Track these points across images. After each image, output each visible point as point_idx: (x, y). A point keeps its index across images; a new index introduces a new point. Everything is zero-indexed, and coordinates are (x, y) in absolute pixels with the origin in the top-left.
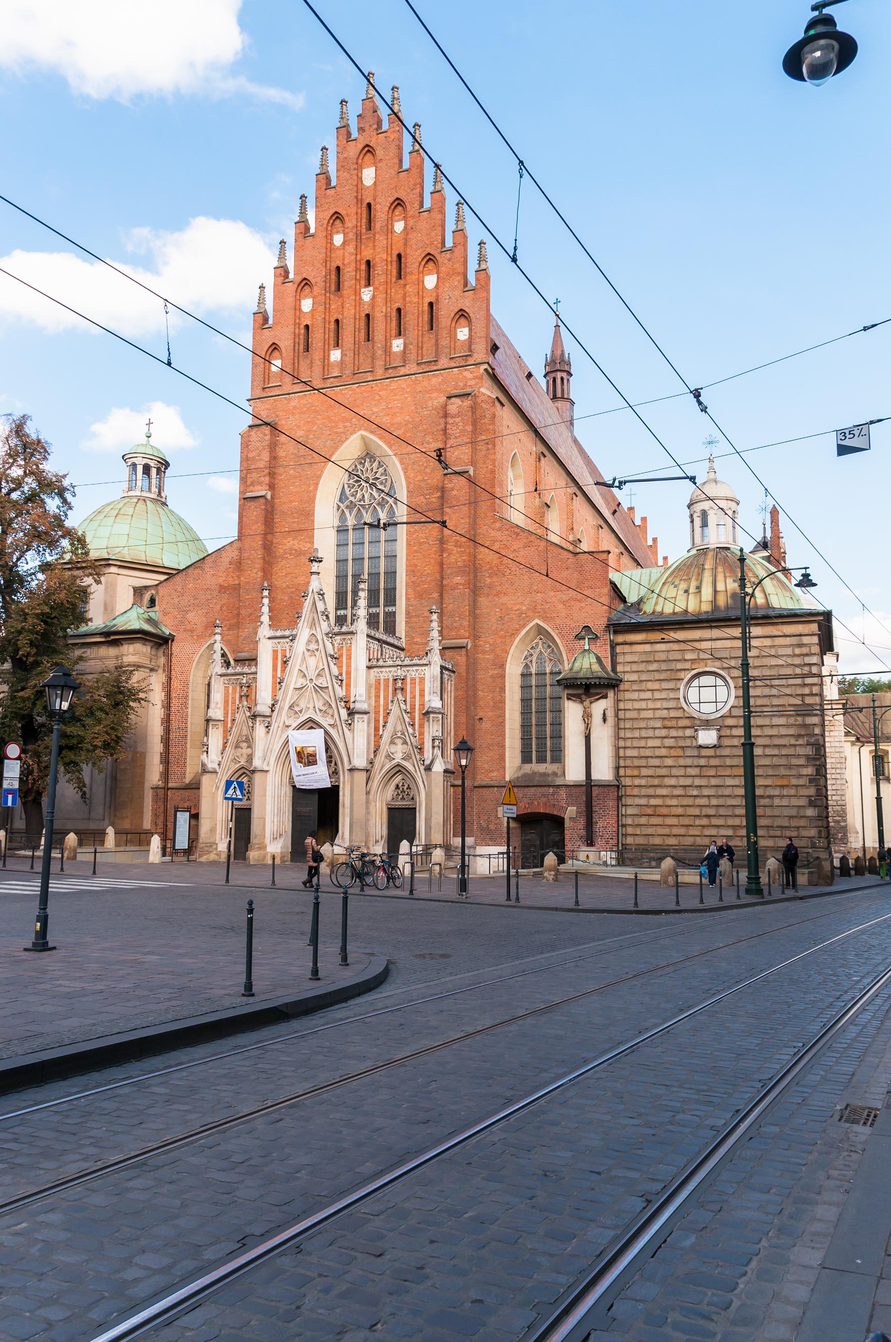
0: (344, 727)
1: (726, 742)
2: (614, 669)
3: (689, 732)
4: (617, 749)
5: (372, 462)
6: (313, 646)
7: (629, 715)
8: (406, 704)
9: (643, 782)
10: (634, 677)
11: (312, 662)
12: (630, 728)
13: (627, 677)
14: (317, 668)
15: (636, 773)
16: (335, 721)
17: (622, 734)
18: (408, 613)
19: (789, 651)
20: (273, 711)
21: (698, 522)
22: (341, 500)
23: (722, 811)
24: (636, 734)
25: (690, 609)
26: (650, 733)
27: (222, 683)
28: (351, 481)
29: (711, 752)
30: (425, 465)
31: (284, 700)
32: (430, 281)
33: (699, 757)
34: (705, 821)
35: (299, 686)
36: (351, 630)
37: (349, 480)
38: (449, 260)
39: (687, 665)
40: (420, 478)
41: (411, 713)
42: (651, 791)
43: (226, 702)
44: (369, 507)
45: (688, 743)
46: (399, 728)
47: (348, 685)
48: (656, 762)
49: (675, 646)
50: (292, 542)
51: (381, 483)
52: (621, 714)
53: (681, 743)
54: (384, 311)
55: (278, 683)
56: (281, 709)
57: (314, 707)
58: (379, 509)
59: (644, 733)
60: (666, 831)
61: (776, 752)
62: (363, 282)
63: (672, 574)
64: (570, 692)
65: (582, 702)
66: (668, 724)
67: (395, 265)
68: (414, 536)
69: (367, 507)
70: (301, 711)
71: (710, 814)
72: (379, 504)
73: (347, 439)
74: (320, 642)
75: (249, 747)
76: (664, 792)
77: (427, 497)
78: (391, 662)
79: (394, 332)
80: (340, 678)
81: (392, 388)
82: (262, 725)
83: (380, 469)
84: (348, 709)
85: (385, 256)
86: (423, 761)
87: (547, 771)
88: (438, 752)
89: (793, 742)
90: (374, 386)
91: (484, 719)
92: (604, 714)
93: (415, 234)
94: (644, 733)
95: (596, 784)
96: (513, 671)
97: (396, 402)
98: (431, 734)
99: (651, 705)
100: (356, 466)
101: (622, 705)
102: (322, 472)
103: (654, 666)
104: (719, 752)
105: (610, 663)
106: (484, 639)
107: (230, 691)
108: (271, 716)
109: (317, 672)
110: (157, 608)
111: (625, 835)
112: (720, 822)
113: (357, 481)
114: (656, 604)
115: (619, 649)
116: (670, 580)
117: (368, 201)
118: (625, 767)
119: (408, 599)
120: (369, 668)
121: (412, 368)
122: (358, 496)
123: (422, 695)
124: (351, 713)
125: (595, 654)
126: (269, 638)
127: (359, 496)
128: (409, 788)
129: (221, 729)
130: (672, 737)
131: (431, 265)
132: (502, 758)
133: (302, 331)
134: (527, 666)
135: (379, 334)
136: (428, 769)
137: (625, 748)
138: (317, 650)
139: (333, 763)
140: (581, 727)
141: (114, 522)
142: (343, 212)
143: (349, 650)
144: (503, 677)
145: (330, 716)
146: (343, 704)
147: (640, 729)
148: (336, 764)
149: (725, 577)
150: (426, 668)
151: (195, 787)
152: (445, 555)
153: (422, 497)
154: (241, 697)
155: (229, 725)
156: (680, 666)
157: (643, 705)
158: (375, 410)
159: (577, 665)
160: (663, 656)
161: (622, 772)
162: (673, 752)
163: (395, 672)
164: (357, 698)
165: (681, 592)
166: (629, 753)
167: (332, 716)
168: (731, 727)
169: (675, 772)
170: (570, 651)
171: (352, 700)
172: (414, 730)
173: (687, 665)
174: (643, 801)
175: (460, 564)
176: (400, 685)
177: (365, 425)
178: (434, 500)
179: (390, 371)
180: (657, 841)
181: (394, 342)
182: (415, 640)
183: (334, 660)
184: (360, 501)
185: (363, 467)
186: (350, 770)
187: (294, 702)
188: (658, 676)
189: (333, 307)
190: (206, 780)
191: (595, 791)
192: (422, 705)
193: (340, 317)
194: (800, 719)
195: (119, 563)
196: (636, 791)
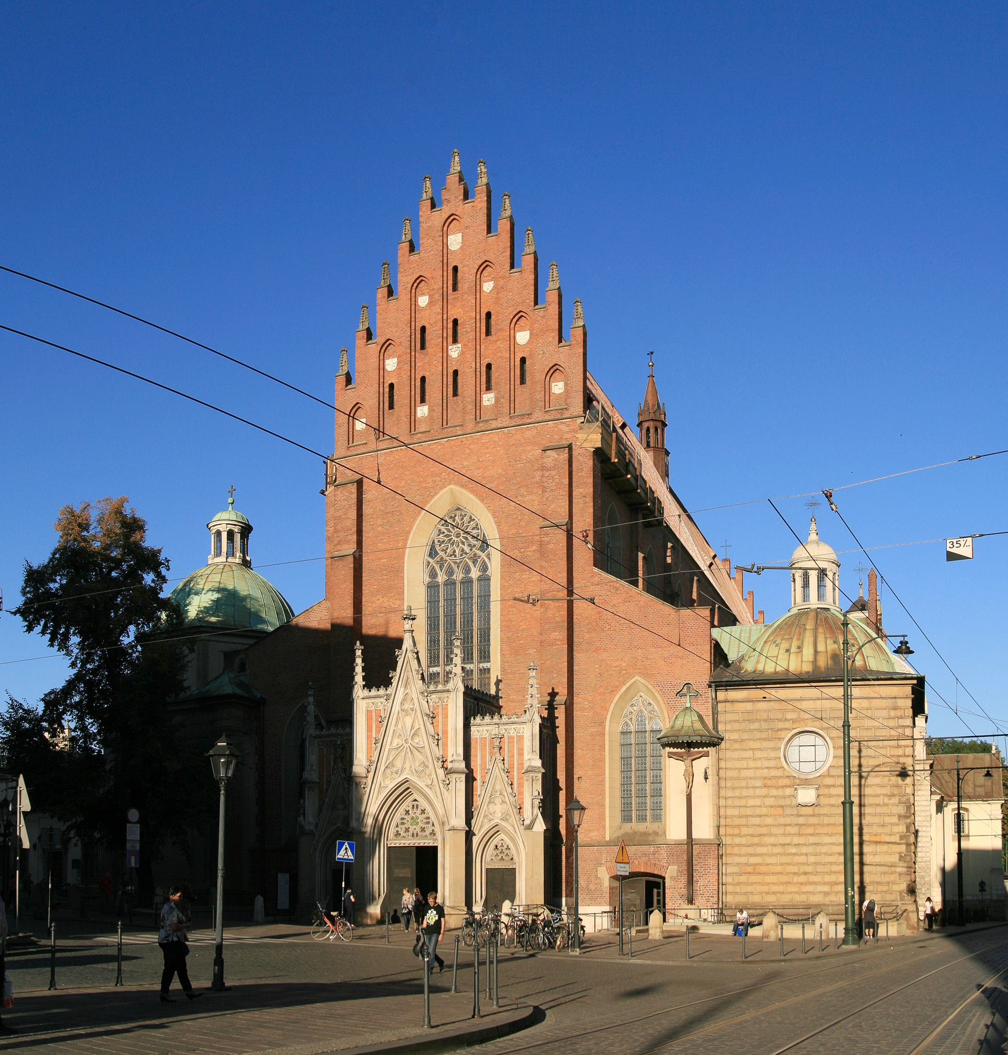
3: (789, 791)
7: (730, 774)
9: (743, 840)
11: (408, 721)
13: (727, 736)
15: (736, 831)
17: (722, 793)
20: (368, 772)
22: (430, 555)
23: (819, 869)
24: (737, 793)
29: (809, 811)
30: (519, 518)
33: (798, 815)
34: (803, 879)
35: (395, 744)
36: (447, 688)
38: (543, 317)
40: (514, 531)
42: (750, 850)
45: (787, 802)
47: (445, 745)
48: (757, 821)
52: (722, 773)
53: (782, 802)
54: (474, 366)
59: (745, 793)
60: (765, 889)
64: (671, 750)
66: (769, 782)
68: (509, 591)
71: (807, 871)
73: (436, 494)
74: (416, 701)
76: (763, 850)
77: (521, 550)
78: (489, 721)
80: (437, 737)
81: (483, 441)
83: (472, 523)
86: (523, 821)
87: (647, 830)
90: (464, 440)
91: (583, 778)
92: (706, 773)
93: (505, 293)
94: (745, 793)
97: (488, 455)
99: (752, 764)
102: (411, 527)
104: (817, 810)
105: (711, 721)
106: (583, 696)
108: (366, 777)
109: (413, 731)
113: (447, 536)
119: (502, 655)
122: (448, 551)
123: (521, 753)
124: (448, 772)
125: (696, 711)
126: (363, 698)
128: (508, 848)
130: (772, 797)
136: (530, 827)
139: (431, 824)
143: (445, 709)
145: (427, 777)
146: (440, 764)
147: (741, 788)
148: (433, 825)
153: (516, 551)
157: (744, 764)
158: (465, 463)
161: (722, 831)
162: (773, 811)
166: (730, 812)
169: (774, 830)
170: (671, 708)
171: (450, 759)
177: (456, 479)
178: (529, 553)
179: (481, 425)
181: (484, 395)
182: (511, 697)
184: (451, 556)
192: (521, 764)
196: (736, 850)
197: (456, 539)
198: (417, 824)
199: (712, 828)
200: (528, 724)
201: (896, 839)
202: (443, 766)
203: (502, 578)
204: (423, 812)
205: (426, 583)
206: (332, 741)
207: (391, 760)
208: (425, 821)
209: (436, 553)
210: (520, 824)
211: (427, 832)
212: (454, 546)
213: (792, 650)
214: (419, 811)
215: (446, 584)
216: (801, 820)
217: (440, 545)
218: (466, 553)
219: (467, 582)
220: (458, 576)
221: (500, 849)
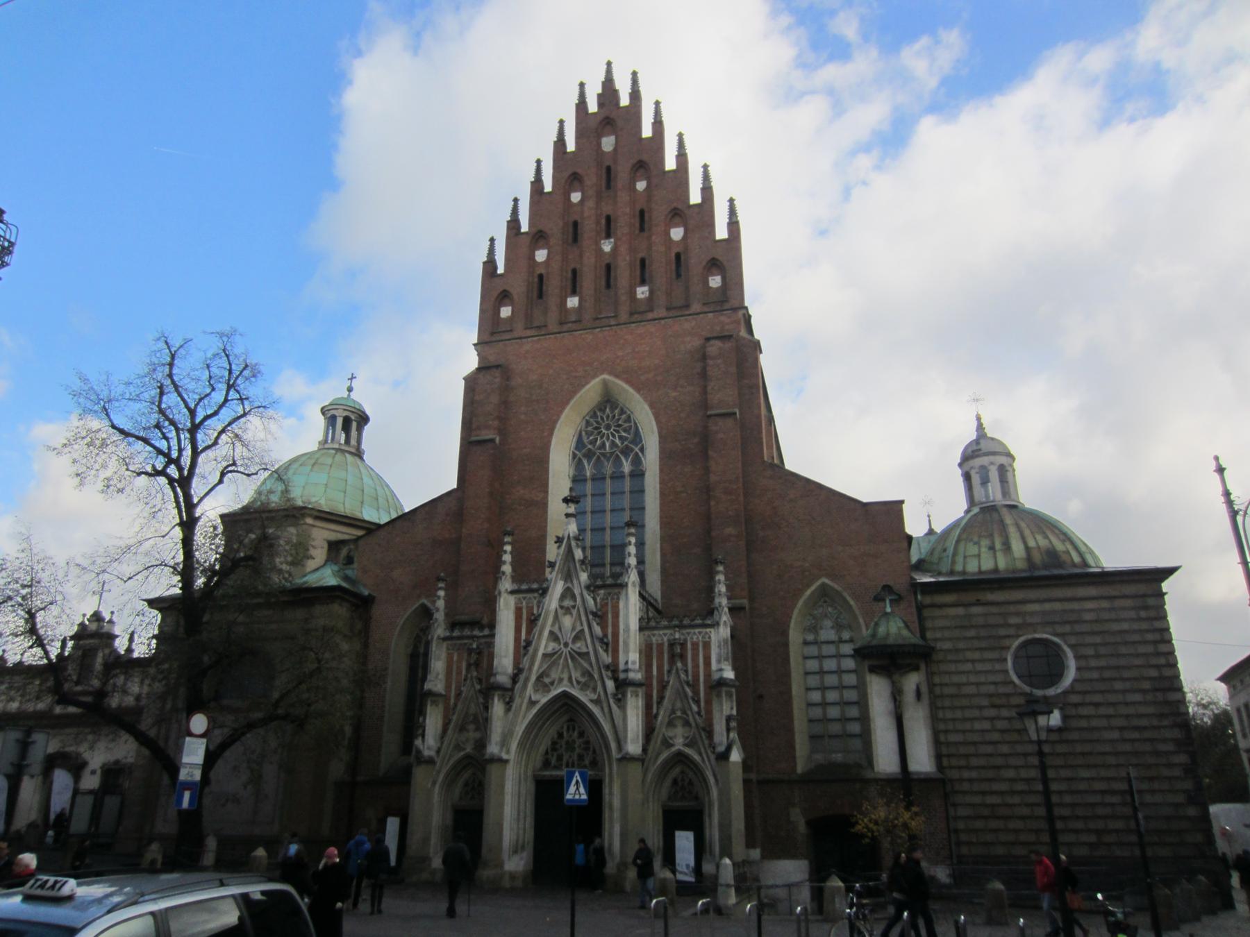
0: (614, 707)
1: (1074, 723)
2: (923, 637)
5: (612, 410)
6: (568, 603)
7: (947, 691)
8: (687, 675)
9: (974, 774)
10: (947, 645)
11: (567, 621)
12: (949, 708)
13: (939, 645)
14: (573, 629)
15: (963, 762)
16: (599, 695)
19: (1132, 614)
22: (577, 448)
24: (959, 714)
26: (976, 713)
27: (444, 649)
30: (679, 409)
31: (530, 669)
32: (677, 234)
35: (550, 650)
36: (619, 582)
37: (587, 427)
39: (1012, 631)
41: (694, 685)
44: (611, 457)
46: (679, 705)
48: (989, 749)
49: (994, 609)
50: (522, 491)
51: (625, 431)
52: (937, 690)
54: (628, 258)
55: (523, 647)
56: (527, 680)
57: (570, 679)
58: (622, 458)
59: (968, 713)
61: (1136, 735)
62: (604, 235)
63: (964, 530)
66: (997, 701)
68: (669, 485)
69: (608, 455)
70: (552, 683)
72: (622, 452)
73: (587, 383)
75: (477, 729)
77: (683, 443)
78: (666, 623)
79: (638, 280)
82: (501, 701)
83: (624, 416)
84: (616, 679)
85: (628, 210)
86: (714, 748)
88: (733, 735)
89: (1155, 722)
94: (968, 713)
95: (915, 777)
98: (724, 713)
100: (595, 413)
101: (937, 680)
103: (972, 633)
107: (455, 658)
108: (512, 690)
109: (574, 634)
110: (355, 565)
111: (959, 844)
112: (1079, 825)
113: (596, 428)
114: (954, 562)
115: (926, 613)
116: (964, 536)
117: (608, 164)
118: (949, 756)
119: (663, 555)
120: (641, 629)
121: (661, 312)
125: (901, 618)
126: (512, 592)
127: (598, 442)
128: (691, 783)
129: (441, 707)
131: (677, 219)
132: (791, 746)
133: (536, 280)
136: (725, 756)
137: (946, 732)
138: (574, 607)
139: (591, 749)
141: (311, 470)
144: (786, 645)
145: (590, 689)
146: (609, 674)
148: (594, 752)
149: (1032, 533)
150: (712, 630)
151: (403, 778)
152: (712, 503)
154: (469, 666)
155: (452, 701)
156: (1002, 632)
158: (620, 353)
159: (882, 630)
160: (981, 621)
163: (671, 634)
164: (630, 666)
165: (984, 550)
166: (953, 738)
167: (595, 690)
168: (1076, 705)
169: (1013, 761)
171: (622, 667)
172: (699, 706)
173: (1012, 631)
174: (977, 800)
175: (730, 513)
176: (679, 651)
179: (636, 316)
180: (1000, 851)
183: (597, 619)
185: (604, 413)
186: (620, 760)
187: (543, 673)
188: (976, 644)
189: (570, 257)
190: (420, 775)
193: (578, 266)
195: (316, 514)
197: (604, 431)
198: (573, 749)
199: (933, 759)
200: (716, 627)
202: (613, 675)
203: (661, 470)
204: (581, 734)
205: (571, 476)
206: (465, 644)
207: (545, 666)
208: (582, 746)
209: (584, 446)
210: (711, 752)
211: (587, 762)
212: (604, 439)
214: (576, 734)
217: (588, 438)
218: (616, 446)
219: (618, 476)
220: (608, 469)
221: (680, 784)
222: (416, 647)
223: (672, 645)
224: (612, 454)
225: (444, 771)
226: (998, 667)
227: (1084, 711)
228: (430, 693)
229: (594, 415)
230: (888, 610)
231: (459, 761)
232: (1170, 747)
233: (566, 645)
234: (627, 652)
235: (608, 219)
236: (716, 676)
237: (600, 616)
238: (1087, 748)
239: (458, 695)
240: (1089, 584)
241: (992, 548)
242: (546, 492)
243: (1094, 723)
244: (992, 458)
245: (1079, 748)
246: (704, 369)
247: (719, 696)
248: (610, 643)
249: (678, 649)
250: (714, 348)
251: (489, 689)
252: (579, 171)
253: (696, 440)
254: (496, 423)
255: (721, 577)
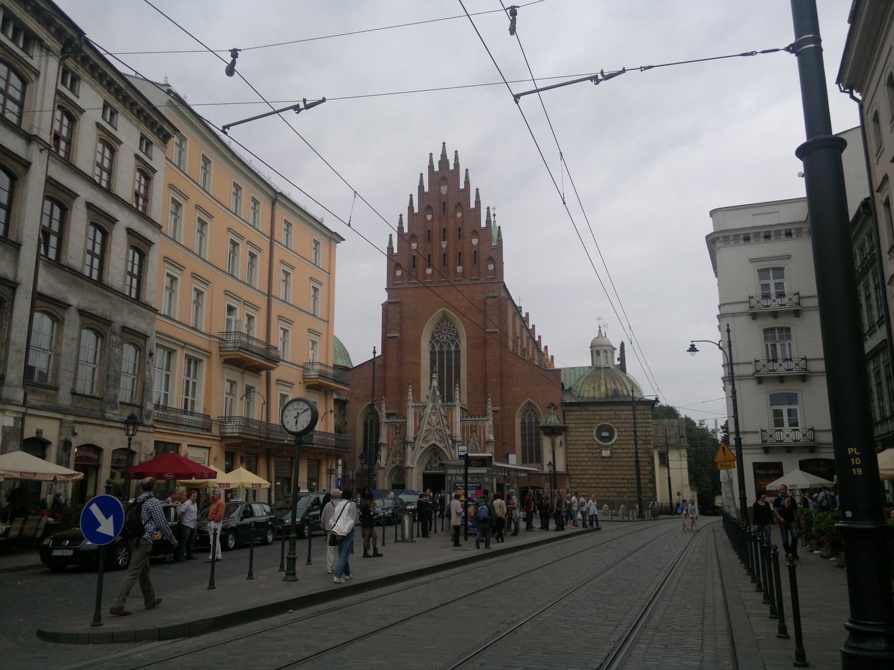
0: (451, 449)
1: (614, 455)
2: (564, 423)
3: (598, 451)
4: (567, 457)
5: (447, 321)
7: (572, 442)
9: (578, 472)
10: (573, 426)
11: (434, 418)
13: (570, 426)
14: (436, 421)
15: (575, 468)
18: (468, 394)
20: (415, 440)
21: (595, 355)
24: (575, 451)
25: (596, 396)
26: (581, 451)
28: (437, 330)
29: (608, 460)
32: (475, 242)
34: (606, 490)
35: (427, 429)
43: (388, 434)
45: (598, 455)
46: (474, 448)
47: (452, 429)
48: (584, 463)
49: (591, 413)
53: (595, 455)
56: (420, 439)
57: (435, 439)
62: (442, 239)
63: (586, 379)
65: (551, 436)
66: (589, 447)
67: (457, 233)
73: (436, 311)
74: (438, 409)
75: (400, 456)
79: (458, 263)
84: (452, 440)
85: (453, 228)
94: (578, 451)
96: (518, 421)
99: (581, 438)
101: (568, 438)
103: (582, 421)
108: (414, 443)
115: (566, 413)
119: (467, 387)
124: (454, 442)
127: (441, 337)
129: (386, 448)
131: (475, 235)
134: (523, 419)
135: (451, 264)
137: (570, 457)
140: (551, 448)
142: (432, 206)
144: (514, 425)
152: (487, 369)
154: (396, 433)
156: (593, 421)
158: (450, 299)
159: (549, 420)
160: (585, 417)
161: (569, 468)
165: (591, 388)
166: (572, 459)
167: (444, 443)
168: (616, 449)
171: (454, 435)
188: (583, 426)
191: (558, 477)
192: (484, 438)
193: (431, 254)
194: (645, 446)
196: (575, 477)
201: (647, 472)
213: (596, 388)
215: (439, 352)
216: (604, 464)
219: (449, 352)
220: (445, 349)
222: (366, 421)
223: (472, 427)
224: (447, 342)
225: (389, 471)
226: (590, 434)
227: (618, 451)
228: (381, 444)
229: (439, 324)
230: (552, 412)
231: (395, 467)
232: (646, 464)
233: (434, 427)
234: (456, 430)
235: (444, 230)
236: (487, 439)
237: (446, 417)
238: (618, 464)
239: (393, 444)
240: (626, 405)
241: (594, 388)
242: (420, 359)
243: (622, 455)
244: (602, 347)
245: (615, 464)
246: (486, 308)
247: (488, 445)
248: (450, 427)
249: (474, 429)
250: (489, 302)
251: (405, 443)
252: (430, 204)
253: (481, 340)
254: (398, 328)
255: (489, 403)
